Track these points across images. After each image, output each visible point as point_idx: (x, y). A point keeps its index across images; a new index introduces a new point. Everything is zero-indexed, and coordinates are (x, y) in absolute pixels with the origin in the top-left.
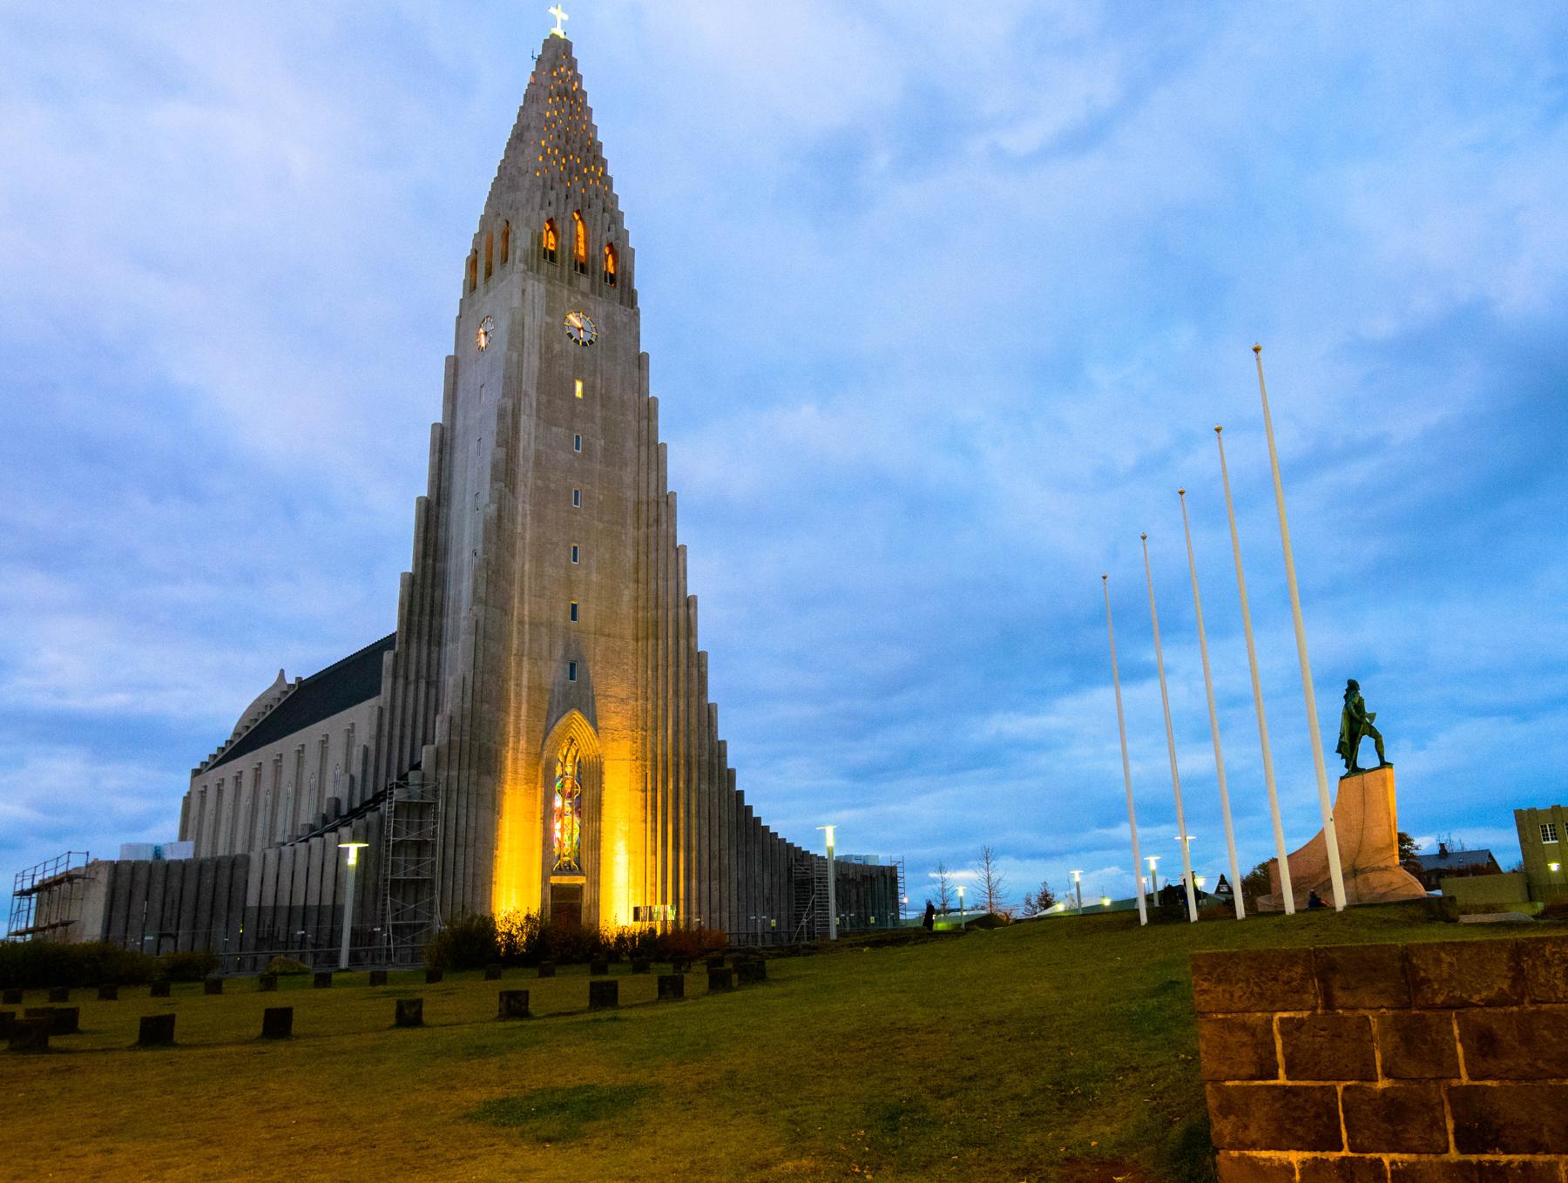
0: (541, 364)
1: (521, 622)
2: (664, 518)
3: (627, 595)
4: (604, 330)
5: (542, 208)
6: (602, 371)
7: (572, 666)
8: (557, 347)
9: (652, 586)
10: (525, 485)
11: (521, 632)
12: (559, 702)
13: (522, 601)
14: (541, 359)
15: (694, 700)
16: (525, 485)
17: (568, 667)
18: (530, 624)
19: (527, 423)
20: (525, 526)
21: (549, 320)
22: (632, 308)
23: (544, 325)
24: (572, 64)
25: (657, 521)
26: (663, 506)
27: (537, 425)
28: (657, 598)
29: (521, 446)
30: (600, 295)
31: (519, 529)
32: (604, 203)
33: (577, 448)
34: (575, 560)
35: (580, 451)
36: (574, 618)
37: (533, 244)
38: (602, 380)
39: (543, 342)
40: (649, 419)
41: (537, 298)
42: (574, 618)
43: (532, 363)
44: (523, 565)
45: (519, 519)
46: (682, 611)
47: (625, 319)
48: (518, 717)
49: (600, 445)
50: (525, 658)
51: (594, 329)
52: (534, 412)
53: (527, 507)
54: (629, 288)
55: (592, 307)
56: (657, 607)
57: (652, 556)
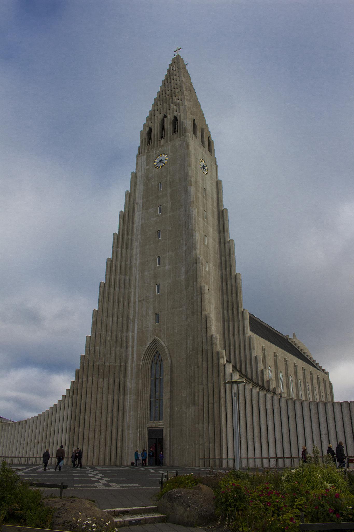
0: (144, 187)
1: (135, 303)
3: (183, 270)
4: (171, 154)
6: (170, 172)
8: (151, 175)
10: (137, 242)
11: (134, 308)
12: (150, 335)
13: (135, 292)
14: (144, 185)
15: (199, 314)
16: (137, 242)
17: (155, 317)
18: (139, 301)
20: (136, 260)
21: (148, 167)
23: (145, 171)
27: (142, 213)
29: (136, 225)
30: (170, 141)
31: (134, 262)
36: (158, 292)
38: (170, 176)
39: (145, 177)
41: (143, 163)
43: (140, 188)
44: (136, 275)
45: (135, 257)
47: (180, 142)
48: (133, 347)
49: (170, 205)
50: (136, 320)
52: (141, 208)
53: (138, 250)
54: (183, 127)
55: (165, 149)
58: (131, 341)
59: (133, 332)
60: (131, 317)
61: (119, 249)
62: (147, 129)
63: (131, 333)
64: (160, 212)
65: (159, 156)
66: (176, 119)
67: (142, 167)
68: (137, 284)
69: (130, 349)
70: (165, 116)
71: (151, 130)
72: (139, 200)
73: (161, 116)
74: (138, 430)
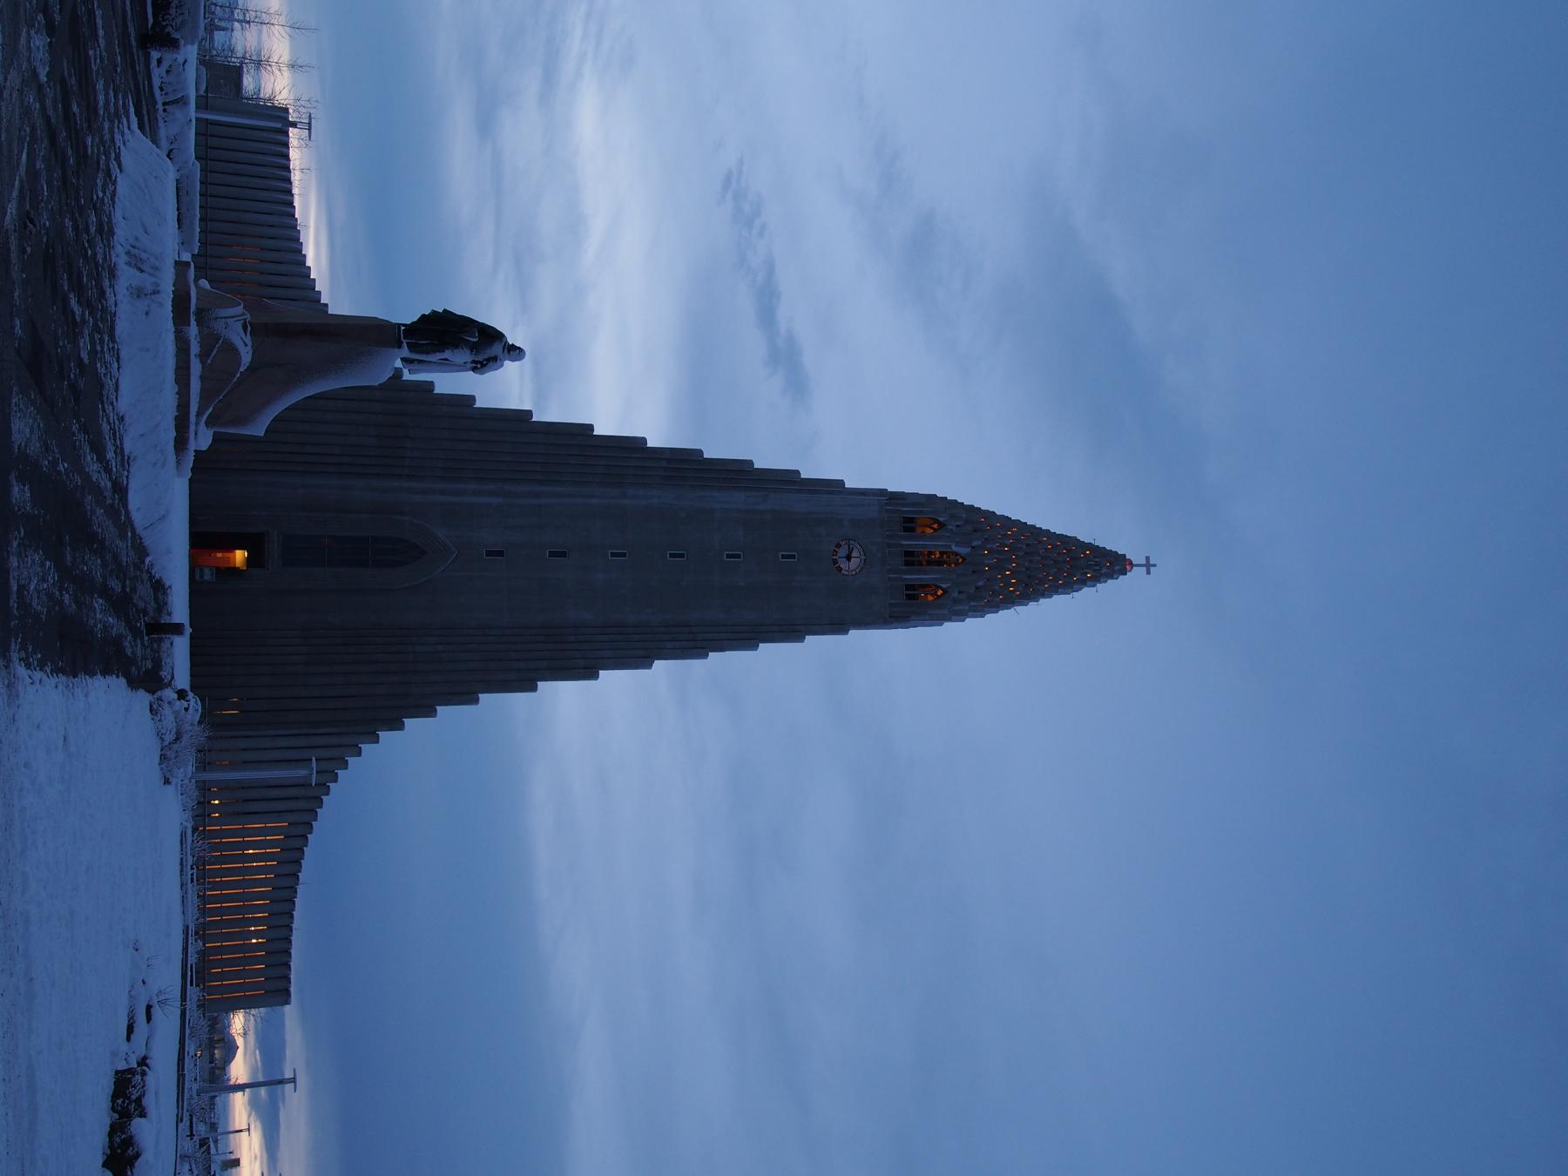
7: (500, 553)
22: (890, 617)
33: (728, 556)
34: (613, 555)
36: (552, 554)
42: (552, 554)
51: (854, 573)
64: (728, 556)
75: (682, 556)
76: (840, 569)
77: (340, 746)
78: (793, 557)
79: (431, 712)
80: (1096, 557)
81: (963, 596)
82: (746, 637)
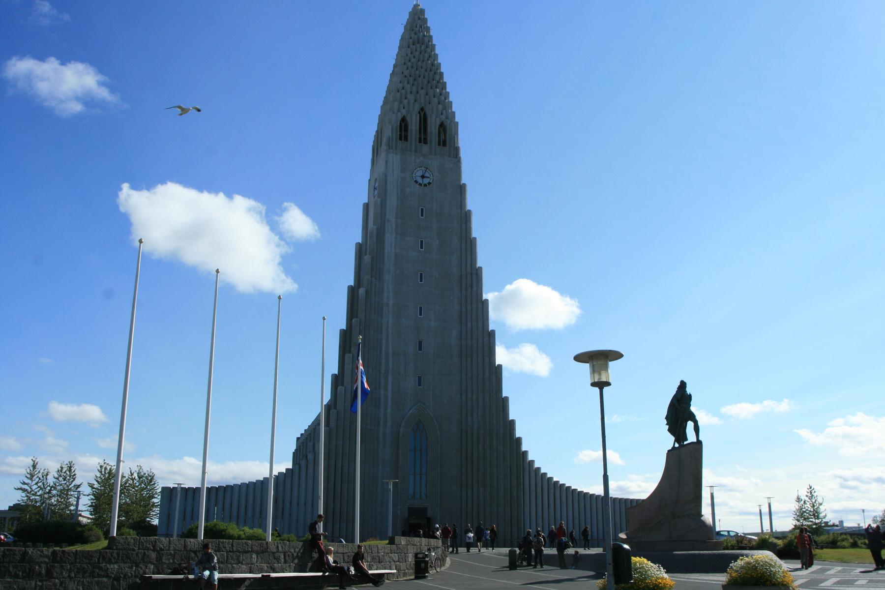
1: (387, 354)
2: (474, 285)
5: (399, 111)
7: (420, 378)
9: (469, 326)
19: (390, 238)
22: (456, 158)
24: (425, 21)
25: (472, 286)
26: (474, 276)
27: (396, 238)
28: (472, 332)
29: (386, 251)
30: (435, 155)
32: (439, 98)
33: (422, 247)
34: (421, 314)
35: (423, 250)
36: (420, 349)
37: (392, 133)
40: (466, 224)
42: (420, 349)
43: (392, 201)
45: (385, 294)
46: (486, 339)
48: (386, 409)
50: (390, 376)
51: (431, 175)
56: (472, 338)
57: (469, 307)
58: (382, 399)
59: (386, 390)
60: (383, 372)
61: (374, 279)
62: (400, 118)
63: (382, 391)
64: (422, 247)
65: (421, 168)
66: (442, 125)
67: (393, 170)
68: (390, 331)
69: (382, 410)
70: (422, 109)
71: (404, 120)
72: (391, 216)
73: (417, 107)
74: (399, 507)
75: (421, 275)
76: (429, 183)
77: (529, 470)
78: (422, 210)
79: (513, 422)
80: (417, 27)
81: (444, 112)
82: (469, 246)
